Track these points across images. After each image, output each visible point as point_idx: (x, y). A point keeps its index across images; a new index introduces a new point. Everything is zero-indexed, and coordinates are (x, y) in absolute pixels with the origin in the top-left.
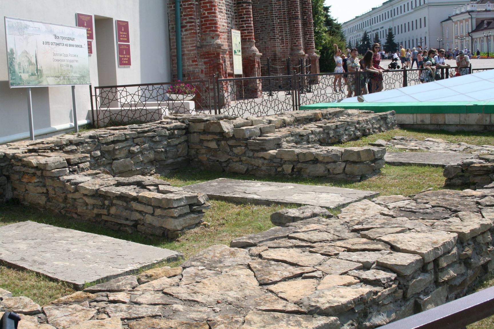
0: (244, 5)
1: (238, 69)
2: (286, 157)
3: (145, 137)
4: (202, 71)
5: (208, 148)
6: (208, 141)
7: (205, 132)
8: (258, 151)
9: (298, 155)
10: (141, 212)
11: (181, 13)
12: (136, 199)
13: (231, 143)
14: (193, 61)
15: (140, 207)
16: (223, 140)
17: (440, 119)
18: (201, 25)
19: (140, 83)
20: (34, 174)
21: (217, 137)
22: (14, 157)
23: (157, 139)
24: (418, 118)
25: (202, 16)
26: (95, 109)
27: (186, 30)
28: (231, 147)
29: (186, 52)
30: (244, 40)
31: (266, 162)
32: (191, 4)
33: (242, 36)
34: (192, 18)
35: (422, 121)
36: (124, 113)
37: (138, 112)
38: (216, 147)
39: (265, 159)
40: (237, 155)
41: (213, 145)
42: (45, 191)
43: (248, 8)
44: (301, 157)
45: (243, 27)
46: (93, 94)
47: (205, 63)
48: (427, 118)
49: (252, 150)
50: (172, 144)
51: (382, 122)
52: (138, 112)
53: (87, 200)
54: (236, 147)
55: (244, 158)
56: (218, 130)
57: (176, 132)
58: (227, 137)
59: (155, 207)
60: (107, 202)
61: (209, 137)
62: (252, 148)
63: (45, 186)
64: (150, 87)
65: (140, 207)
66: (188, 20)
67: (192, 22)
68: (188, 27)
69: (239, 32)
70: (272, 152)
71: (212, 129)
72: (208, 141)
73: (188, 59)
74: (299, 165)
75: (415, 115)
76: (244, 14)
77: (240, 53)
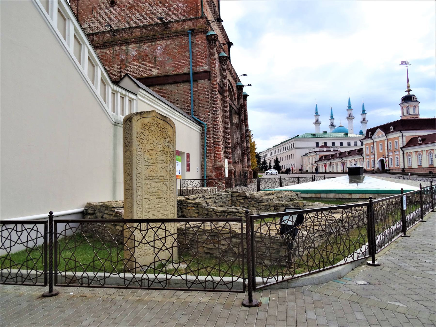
1: (227, 176)
2: (272, 205)
4: (214, 175)
5: (240, 202)
6: (240, 199)
7: (238, 196)
8: (260, 203)
9: (276, 204)
10: (240, 217)
11: (207, 151)
12: (238, 212)
13: (249, 200)
14: (211, 171)
15: (239, 215)
16: (246, 199)
17: (318, 195)
18: (214, 156)
20: (193, 206)
21: (244, 198)
22: (183, 201)
23: (223, 198)
24: (309, 195)
25: (215, 153)
26: (181, 189)
27: (208, 158)
28: (249, 201)
29: (208, 167)
30: (229, 164)
31: (264, 207)
35: (311, 196)
36: (193, 190)
37: (199, 190)
38: (243, 201)
39: (263, 206)
40: (251, 204)
41: (242, 201)
42: (198, 212)
44: (277, 205)
46: (181, 182)
47: (216, 172)
48: (313, 195)
49: (258, 203)
50: (227, 200)
51: (296, 196)
52: (199, 190)
53: (218, 214)
54: (251, 201)
55: (255, 206)
56: (245, 196)
57: (228, 196)
60: (226, 214)
61: (241, 198)
62: (258, 202)
63: (198, 210)
64: (190, 181)
65: (239, 215)
66: (209, 154)
68: (209, 157)
70: (266, 203)
71: (242, 195)
72: (240, 199)
73: (209, 170)
74: (277, 208)
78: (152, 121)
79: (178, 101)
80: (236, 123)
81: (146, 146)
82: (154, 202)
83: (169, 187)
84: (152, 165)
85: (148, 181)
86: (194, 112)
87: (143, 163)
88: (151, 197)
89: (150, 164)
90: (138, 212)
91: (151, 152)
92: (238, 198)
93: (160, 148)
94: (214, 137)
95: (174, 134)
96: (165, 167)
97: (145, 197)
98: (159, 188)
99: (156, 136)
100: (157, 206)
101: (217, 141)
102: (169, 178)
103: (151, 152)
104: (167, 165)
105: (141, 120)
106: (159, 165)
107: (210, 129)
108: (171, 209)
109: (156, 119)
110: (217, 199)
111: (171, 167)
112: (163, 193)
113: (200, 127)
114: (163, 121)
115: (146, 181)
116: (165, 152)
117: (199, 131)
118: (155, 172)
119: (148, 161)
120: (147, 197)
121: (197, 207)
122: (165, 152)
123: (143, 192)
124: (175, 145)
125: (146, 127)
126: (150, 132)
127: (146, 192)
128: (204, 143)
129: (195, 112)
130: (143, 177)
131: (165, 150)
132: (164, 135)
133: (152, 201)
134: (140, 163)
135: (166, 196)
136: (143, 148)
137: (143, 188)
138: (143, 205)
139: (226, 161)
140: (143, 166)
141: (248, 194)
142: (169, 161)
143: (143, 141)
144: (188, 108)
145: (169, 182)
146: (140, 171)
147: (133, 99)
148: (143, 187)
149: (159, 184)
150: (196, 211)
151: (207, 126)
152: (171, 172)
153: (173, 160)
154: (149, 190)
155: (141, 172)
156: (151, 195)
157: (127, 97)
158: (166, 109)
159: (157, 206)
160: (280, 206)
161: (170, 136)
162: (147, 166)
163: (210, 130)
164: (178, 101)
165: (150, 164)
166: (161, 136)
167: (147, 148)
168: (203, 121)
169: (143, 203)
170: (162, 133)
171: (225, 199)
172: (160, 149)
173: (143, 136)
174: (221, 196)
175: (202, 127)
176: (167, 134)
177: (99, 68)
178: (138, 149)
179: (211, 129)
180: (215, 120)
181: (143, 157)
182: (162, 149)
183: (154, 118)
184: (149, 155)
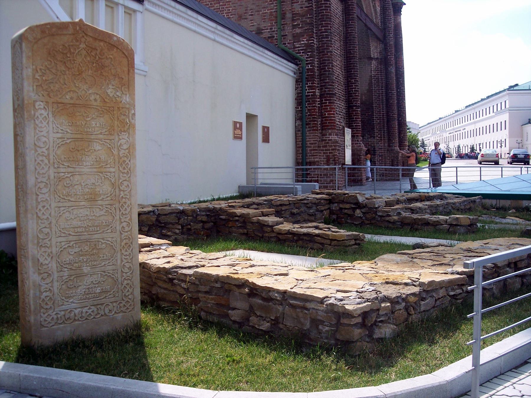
0: (355, 108)
2: (407, 221)
3: (302, 203)
6: (345, 209)
12: (318, 235)
19: (286, 166)
22: (221, 209)
27: (309, 127)
32: (314, 106)
33: (352, 133)
34: (315, 118)
39: (390, 222)
43: (357, 111)
45: (353, 126)
53: (280, 237)
56: (355, 201)
58: (361, 206)
59: (332, 240)
61: (347, 206)
67: (315, 121)
69: (350, 130)
70: (396, 218)
75: (498, 200)
76: (354, 116)
77: (350, 148)
79: (252, 15)
80: (377, 58)
86: (283, 36)
92: (341, 206)
94: (321, 86)
95: (131, 71)
101: (327, 94)
105: (46, 40)
107: (313, 69)
110: (297, 208)
113: (293, 65)
117: (292, 74)
121: (244, 222)
122: (108, 108)
128: (301, 96)
129: (286, 35)
134: (42, 134)
139: (348, 133)
141: (361, 199)
144: (271, 29)
146: (44, 150)
147: (135, 11)
150: (241, 231)
151: (307, 64)
156: (72, 200)
157: (120, 7)
158: (213, 30)
160: (422, 225)
163: (313, 72)
164: (252, 15)
168: (300, 53)
171: (314, 208)
174: (305, 202)
175: (296, 64)
179: (316, 69)
180: (324, 52)
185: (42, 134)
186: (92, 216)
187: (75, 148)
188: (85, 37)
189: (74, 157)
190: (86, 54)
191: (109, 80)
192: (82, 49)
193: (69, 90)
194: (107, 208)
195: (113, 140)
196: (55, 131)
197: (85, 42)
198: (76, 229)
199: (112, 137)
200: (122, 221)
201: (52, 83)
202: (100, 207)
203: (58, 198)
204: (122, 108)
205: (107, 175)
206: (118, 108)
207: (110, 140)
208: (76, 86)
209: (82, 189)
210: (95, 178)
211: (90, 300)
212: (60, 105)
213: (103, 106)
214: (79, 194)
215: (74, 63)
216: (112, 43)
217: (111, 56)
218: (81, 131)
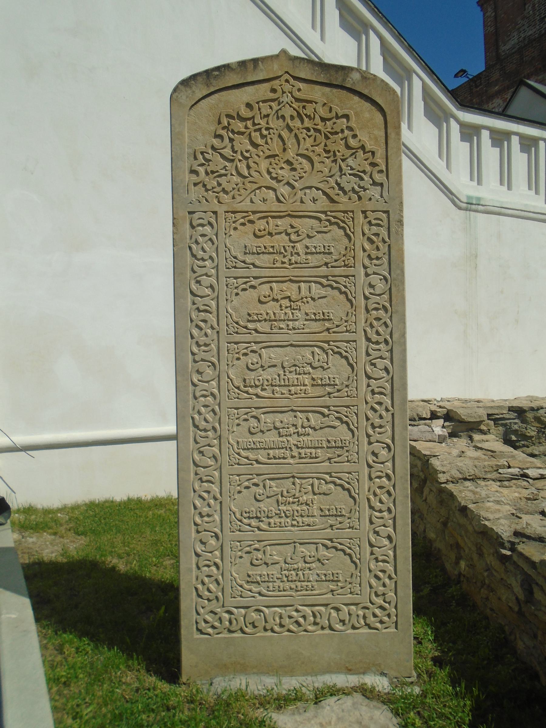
78: (272, 96)
81: (239, 199)
82: (278, 424)
83: (361, 365)
84: (272, 272)
85: (248, 338)
87: (222, 268)
88: (266, 402)
89: (255, 272)
90: (197, 457)
91: (261, 225)
93: (314, 200)
96: (342, 280)
97: (230, 403)
98: (309, 369)
99: (291, 154)
100: (293, 440)
102: (362, 324)
103: (261, 225)
104: (351, 271)
106: (306, 272)
108: (370, 458)
109: (287, 87)
111: (375, 279)
112: (328, 389)
114: (327, 90)
115: (237, 338)
116: (340, 215)
118: (286, 303)
119: (249, 259)
120: (242, 403)
122: (340, 215)
123: (223, 383)
124: (399, 182)
125: (240, 126)
126: (260, 141)
127: (238, 382)
130: (223, 322)
131: (341, 207)
132: (332, 147)
133: (269, 419)
135: (347, 401)
136: (220, 210)
137: (223, 367)
138: (225, 434)
140: (223, 280)
142: (360, 254)
143: (222, 180)
145: (363, 343)
146: (206, 300)
148: (223, 362)
149: (307, 353)
152: (370, 302)
153: (384, 248)
154: (253, 375)
155: (213, 304)
156: (263, 394)
159: (293, 440)
161: (368, 147)
162: (240, 281)
165: (255, 272)
166: (319, 149)
167: (239, 207)
169: (225, 427)
170: (321, 138)
172: (311, 206)
173: (218, 163)
176: (352, 142)
177: (414, 76)
178: (196, 216)
181: (222, 248)
182: (323, 203)
183: (276, 84)
184: (251, 236)
185: (204, 273)
186: (304, 428)
187: (269, 296)
188: (292, 81)
189: (267, 314)
190: (295, 114)
191: (343, 160)
192: (284, 106)
193: (256, 186)
194: (337, 412)
195: (354, 276)
196: (230, 264)
197: (291, 93)
198: (271, 452)
199: (351, 271)
200: (372, 439)
201: (226, 175)
202: (326, 411)
203: (236, 390)
204: (373, 211)
205: (338, 347)
206: (364, 212)
207: (346, 277)
208: (272, 178)
209: (285, 375)
210: (313, 353)
211: (299, 593)
212: (239, 215)
213: (331, 212)
214: (278, 383)
215: (269, 134)
216: (348, 86)
217: (346, 112)
218: (283, 263)
